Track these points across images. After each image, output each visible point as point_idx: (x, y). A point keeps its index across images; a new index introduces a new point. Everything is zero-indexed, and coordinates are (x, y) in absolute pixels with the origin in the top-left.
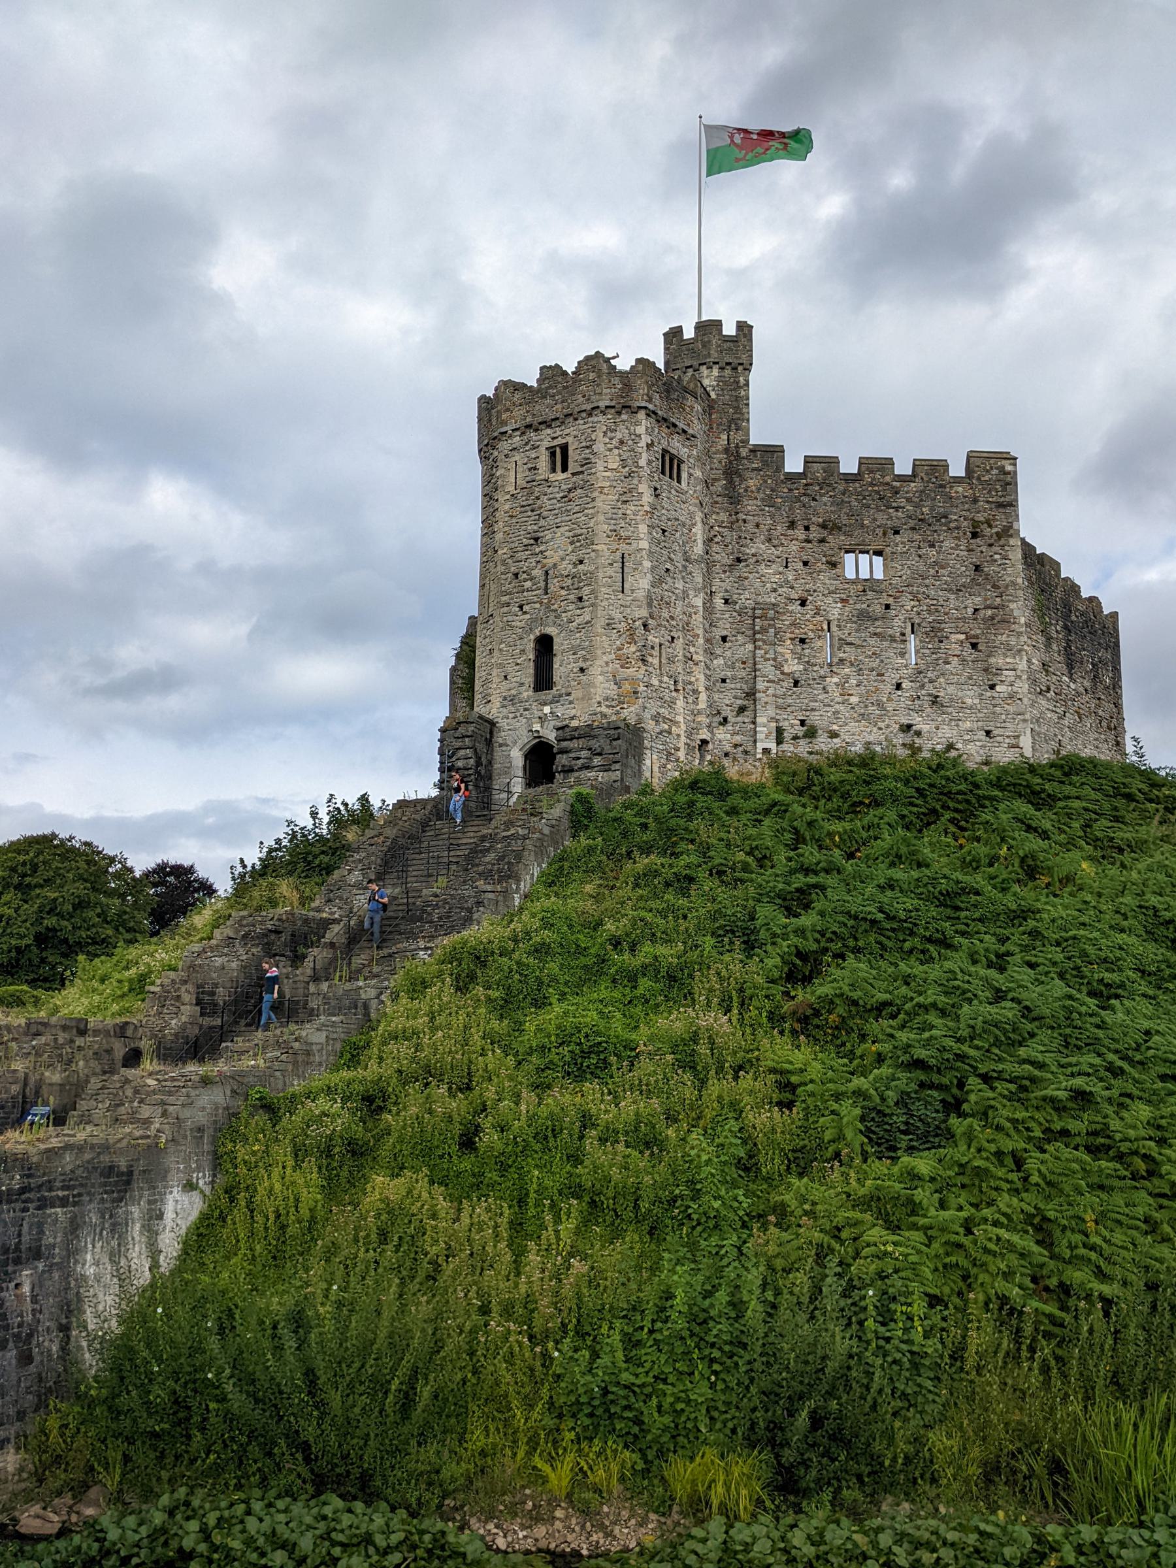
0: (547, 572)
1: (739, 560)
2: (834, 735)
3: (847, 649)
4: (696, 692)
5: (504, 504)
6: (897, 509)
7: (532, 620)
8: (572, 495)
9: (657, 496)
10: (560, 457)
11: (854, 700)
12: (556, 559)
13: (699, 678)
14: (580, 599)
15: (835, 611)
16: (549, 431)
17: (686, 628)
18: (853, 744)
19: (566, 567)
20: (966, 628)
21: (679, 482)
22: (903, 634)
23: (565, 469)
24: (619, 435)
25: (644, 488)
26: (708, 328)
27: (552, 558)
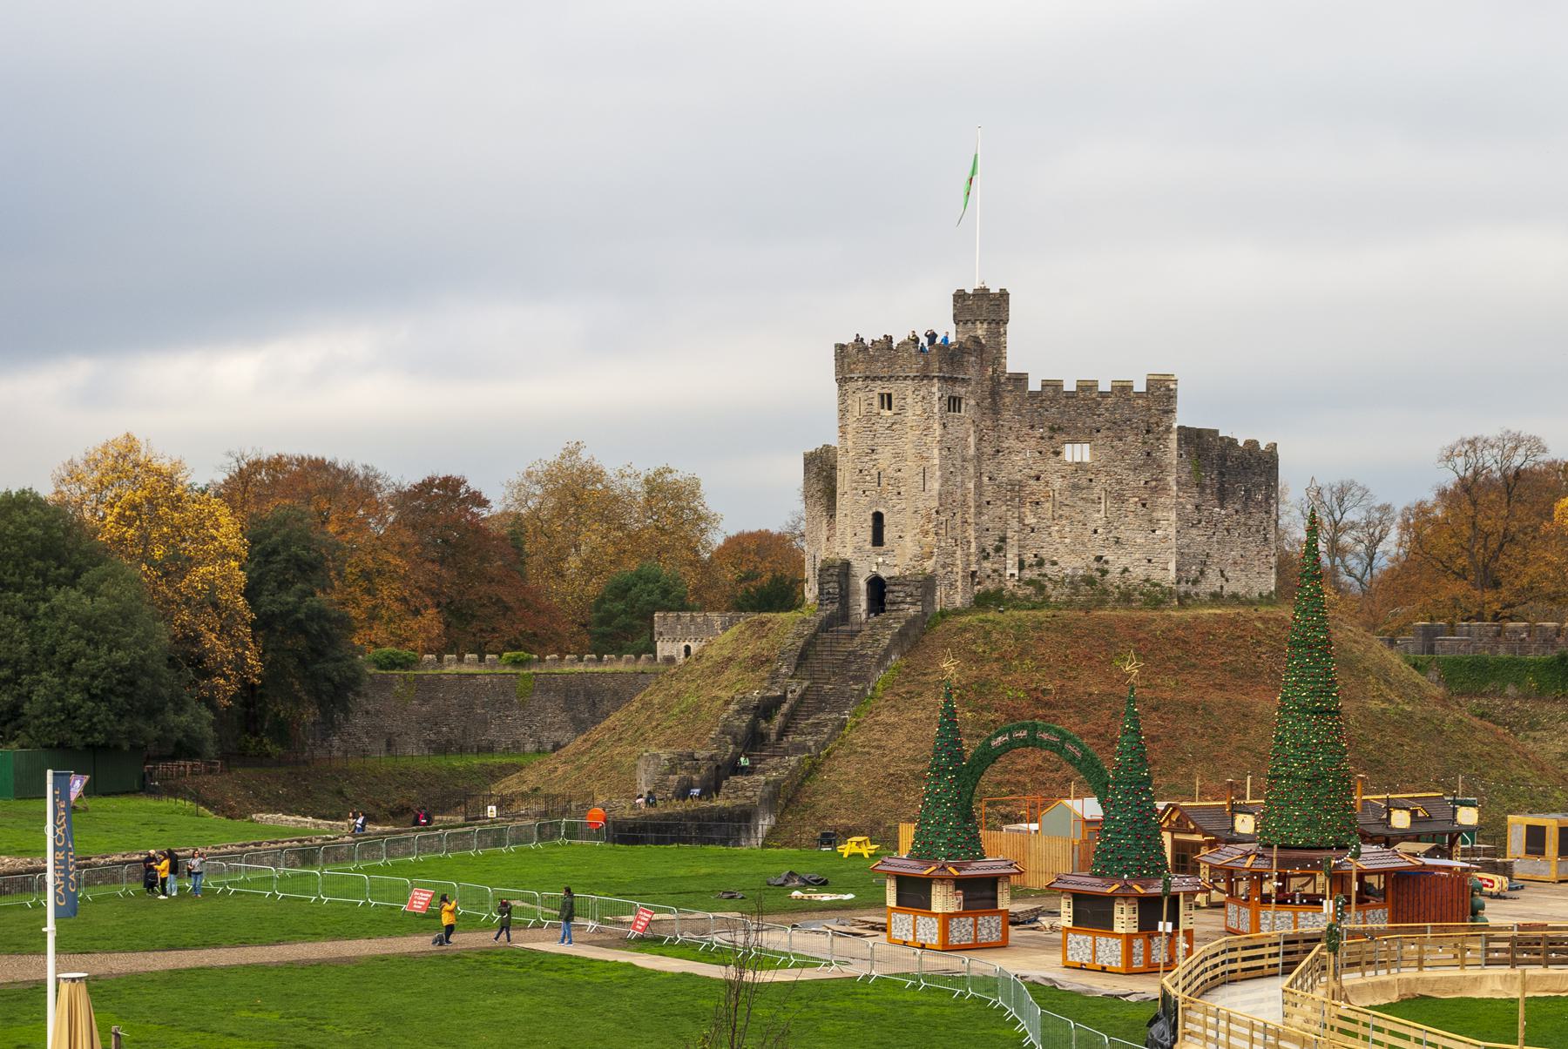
0: (879, 473)
1: (998, 451)
2: (1054, 563)
3: (1064, 508)
4: (969, 542)
5: (852, 425)
6: (1099, 416)
7: (872, 502)
8: (894, 427)
9: (945, 427)
10: (887, 400)
11: (1067, 541)
12: (885, 466)
13: (971, 533)
14: (899, 493)
15: (1058, 483)
16: (879, 382)
17: (964, 503)
18: (1066, 569)
19: (890, 472)
20: (1139, 494)
21: (959, 411)
22: (1100, 498)
23: (890, 408)
24: (921, 393)
25: (936, 426)
26: (982, 294)
27: (883, 464)
